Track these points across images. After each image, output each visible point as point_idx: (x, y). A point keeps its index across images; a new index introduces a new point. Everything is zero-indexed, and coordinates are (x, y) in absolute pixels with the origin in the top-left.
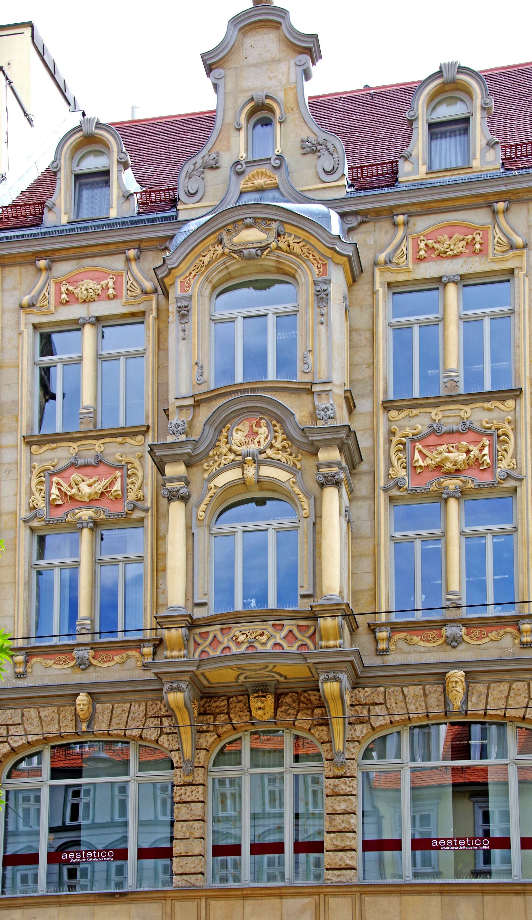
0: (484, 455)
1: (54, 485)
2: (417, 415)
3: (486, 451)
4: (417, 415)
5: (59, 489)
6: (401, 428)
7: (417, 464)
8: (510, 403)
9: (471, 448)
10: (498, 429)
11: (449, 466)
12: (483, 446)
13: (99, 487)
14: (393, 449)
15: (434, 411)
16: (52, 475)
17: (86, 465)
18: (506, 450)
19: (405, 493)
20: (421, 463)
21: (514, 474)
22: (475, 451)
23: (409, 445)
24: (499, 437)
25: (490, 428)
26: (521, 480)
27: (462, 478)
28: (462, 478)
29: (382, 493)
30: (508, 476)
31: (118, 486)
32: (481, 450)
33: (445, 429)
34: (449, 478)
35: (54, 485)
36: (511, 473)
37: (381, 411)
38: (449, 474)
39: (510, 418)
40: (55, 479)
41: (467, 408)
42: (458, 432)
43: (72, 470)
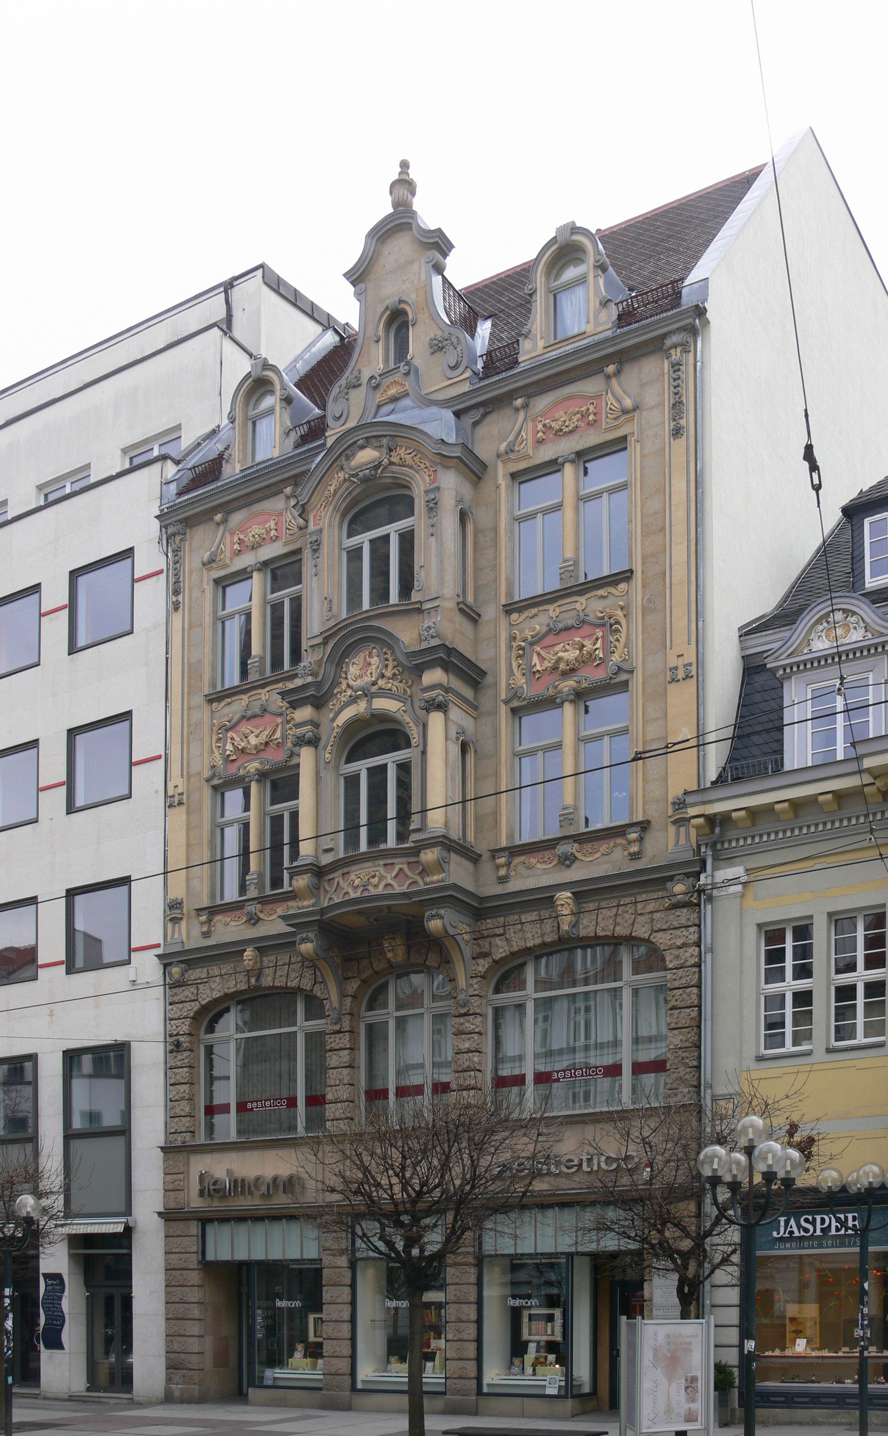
0: (596, 649)
1: (229, 740)
2: (535, 615)
3: (599, 645)
4: (535, 615)
5: (233, 744)
6: (521, 631)
7: (535, 670)
8: (623, 586)
9: (585, 643)
10: (610, 618)
12: (597, 639)
13: (263, 738)
14: (514, 653)
15: (551, 607)
16: (227, 730)
17: (254, 716)
18: (618, 640)
19: (525, 703)
20: (538, 668)
21: (624, 666)
22: (588, 645)
23: (528, 650)
24: (611, 626)
25: (603, 618)
27: (575, 678)
28: (575, 678)
29: (503, 706)
31: (278, 734)
32: (595, 644)
33: (561, 625)
34: (565, 680)
35: (229, 740)
36: (623, 665)
37: (503, 616)
38: (565, 674)
39: (621, 603)
40: (230, 734)
41: (582, 599)
42: (573, 627)
43: (244, 722)
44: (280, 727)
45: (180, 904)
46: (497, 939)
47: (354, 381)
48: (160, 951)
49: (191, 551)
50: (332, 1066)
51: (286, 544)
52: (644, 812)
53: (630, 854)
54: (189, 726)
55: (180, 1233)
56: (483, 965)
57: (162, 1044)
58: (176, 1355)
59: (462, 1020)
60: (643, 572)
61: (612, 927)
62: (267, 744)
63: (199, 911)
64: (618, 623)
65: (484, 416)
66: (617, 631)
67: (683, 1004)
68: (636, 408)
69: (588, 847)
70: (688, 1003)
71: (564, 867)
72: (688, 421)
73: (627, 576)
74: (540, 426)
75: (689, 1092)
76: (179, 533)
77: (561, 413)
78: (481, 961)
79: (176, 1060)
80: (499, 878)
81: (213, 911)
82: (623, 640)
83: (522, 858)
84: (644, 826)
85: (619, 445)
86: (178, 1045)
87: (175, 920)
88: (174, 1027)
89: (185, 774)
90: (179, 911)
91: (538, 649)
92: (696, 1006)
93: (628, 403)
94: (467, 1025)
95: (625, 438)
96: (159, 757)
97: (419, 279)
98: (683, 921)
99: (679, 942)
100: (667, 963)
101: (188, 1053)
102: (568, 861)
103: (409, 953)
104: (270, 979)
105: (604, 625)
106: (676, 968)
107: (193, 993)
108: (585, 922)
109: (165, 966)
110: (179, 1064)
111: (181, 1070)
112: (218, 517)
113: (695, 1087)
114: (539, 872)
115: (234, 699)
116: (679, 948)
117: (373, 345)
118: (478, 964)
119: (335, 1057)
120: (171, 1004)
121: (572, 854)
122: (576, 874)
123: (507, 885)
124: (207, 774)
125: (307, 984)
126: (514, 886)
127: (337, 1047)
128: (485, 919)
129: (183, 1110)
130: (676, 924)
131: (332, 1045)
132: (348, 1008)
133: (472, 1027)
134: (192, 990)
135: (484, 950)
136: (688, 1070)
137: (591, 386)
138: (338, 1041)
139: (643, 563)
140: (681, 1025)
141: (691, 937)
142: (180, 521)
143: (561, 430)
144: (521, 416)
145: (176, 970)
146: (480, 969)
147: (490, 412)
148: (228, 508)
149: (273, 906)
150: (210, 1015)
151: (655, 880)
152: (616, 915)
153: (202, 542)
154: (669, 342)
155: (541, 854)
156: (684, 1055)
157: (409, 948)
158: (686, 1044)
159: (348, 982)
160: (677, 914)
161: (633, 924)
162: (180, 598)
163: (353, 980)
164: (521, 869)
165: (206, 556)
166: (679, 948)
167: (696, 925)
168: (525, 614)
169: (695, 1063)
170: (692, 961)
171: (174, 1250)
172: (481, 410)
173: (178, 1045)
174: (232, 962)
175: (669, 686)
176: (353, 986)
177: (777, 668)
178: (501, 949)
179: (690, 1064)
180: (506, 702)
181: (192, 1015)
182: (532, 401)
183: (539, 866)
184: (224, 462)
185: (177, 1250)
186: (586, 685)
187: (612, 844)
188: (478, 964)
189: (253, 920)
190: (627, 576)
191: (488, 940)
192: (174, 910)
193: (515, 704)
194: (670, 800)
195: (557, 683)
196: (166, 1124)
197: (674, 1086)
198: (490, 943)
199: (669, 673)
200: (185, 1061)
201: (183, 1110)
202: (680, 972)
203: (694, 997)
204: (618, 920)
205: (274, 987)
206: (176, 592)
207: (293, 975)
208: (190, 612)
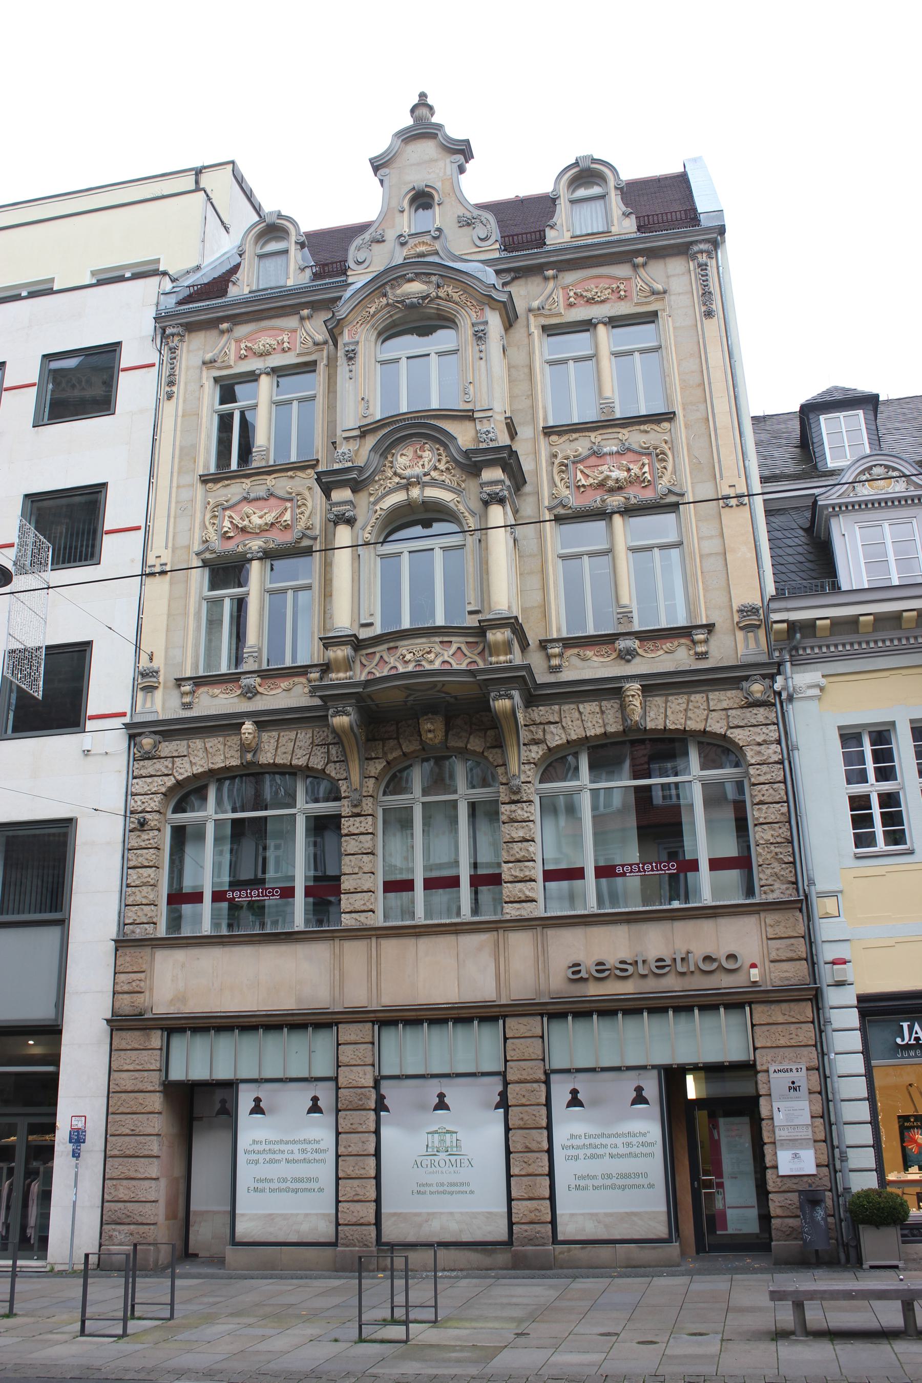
0: (644, 473)
1: (227, 518)
2: (576, 439)
3: (646, 469)
4: (576, 439)
5: (231, 522)
7: (580, 484)
9: (631, 466)
11: (610, 483)
12: (643, 465)
13: (269, 518)
14: (555, 470)
15: (593, 435)
16: (225, 509)
17: (257, 499)
19: (570, 511)
20: (583, 482)
22: (635, 469)
23: (571, 466)
24: (657, 455)
31: (287, 516)
32: (641, 469)
34: (613, 496)
35: (227, 518)
38: (611, 491)
40: (228, 513)
41: (625, 431)
43: (244, 503)
44: (289, 510)
45: (157, 672)
46: (552, 726)
47: (379, 237)
48: (127, 720)
49: (188, 351)
50: (349, 852)
51: (299, 355)
52: (707, 617)
53: (696, 654)
54: (177, 502)
55: (137, 1046)
56: (536, 752)
57: (122, 818)
58: (121, 1205)
59: (513, 807)
60: (684, 416)
61: (683, 721)
62: (272, 524)
63: (179, 682)
64: (663, 453)
65: (513, 279)
66: (664, 460)
67: (770, 800)
68: (665, 292)
69: (650, 644)
70: (777, 799)
71: (623, 662)
72: (716, 306)
73: (669, 417)
74: (572, 294)
75: (787, 889)
76: (179, 334)
77: (593, 286)
78: (534, 748)
79: (139, 840)
80: (550, 667)
81: (199, 682)
82: (670, 468)
83: (575, 651)
84: (710, 628)
85: (651, 317)
86: (142, 824)
87: (150, 689)
88: (139, 803)
89: (170, 545)
90: (155, 680)
91: (582, 467)
92: (784, 802)
93: (659, 287)
94: (520, 812)
95: (655, 314)
96: (138, 528)
97: (445, 172)
98: (761, 719)
99: (759, 739)
100: (749, 758)
101: (156, 833)
102: (627, 656)
103: (446, 735)
104: (269, 755)
105: (650, 454)
106: (758, 764)
107: (167, 767)
108: (652, 714)
109: (132, 737)
110: (143, 844)
111: (146, 851)
112: (225, 326)
113: (793, 883)
114: (596, 665)
115: (233, 481)
116: (759, 744)
117: (398, 215)
118: (530, 751)
119: (353, 842)
120: (134, 778)
121: (635, 649)
122: (638, 667)
123: (559, 675)
124: (197, 547)
125: (317, 762)
126: (567, 675)
127: (356, 832)
128: (537, 706)
129: (145, 897)
130: (754, 722)
131: (350, 829)
132: (371, 790)
133: (526, 815)
134: (166, 763)
135: (537, 737)
136: (784, 866)
137: (622, 271)
138: (357, 825)
140: (770, 821)
141: (771, 734)
142: (181, 325)
143: (593, 299)
144: (551, 284)
145: (147, 742)
146: (533, 755)
147: (519, 278)
148: (236, 319)
149: (277, 681)
150: (187, 793)
151: (728, 678)
152: (686, 710)
153: (196, 349)
154: (695, 248)
155: (597, 648)
156: (777, 850)
157: (448, 729)
158: (779, 840)
159: (371, 762)
160: (755, 712)
161: (706, 720)
162: (175, 389)
163: (377, 761)
164: (575, 661)
165: (208, 357)
166: (759, 744)
167: (774, 724)
169: (791, 859)
170: (776, 758)
171: (126, 1067)
172: (513, 274)
173: (142, 824)
174: (220, 736)
175: (723, 511)
176: (375, 768)
177: (827, 506)
178: (556, 737)
179: (786, 860)
181: (163, 790)
182: (561, 275)
183: (595, 658)
184: (230, 284)
185: (131, 1067)
187: (676, 643)
188: (530, 751)
189: (250, 693)
190: (669, 417)
191: (542, 727)
192: (146, 681)
194: (735, 608)
196: (120, 913)
197: (769, 882)
198: (544, 731)
200: (151, 841)
201: (145, 897)
202: (765, 768)
203: (783, 793)
204: (690, 714)
205: (274, 764)
206: (171, 383)
207: (299, 753)
208: (184, 401)
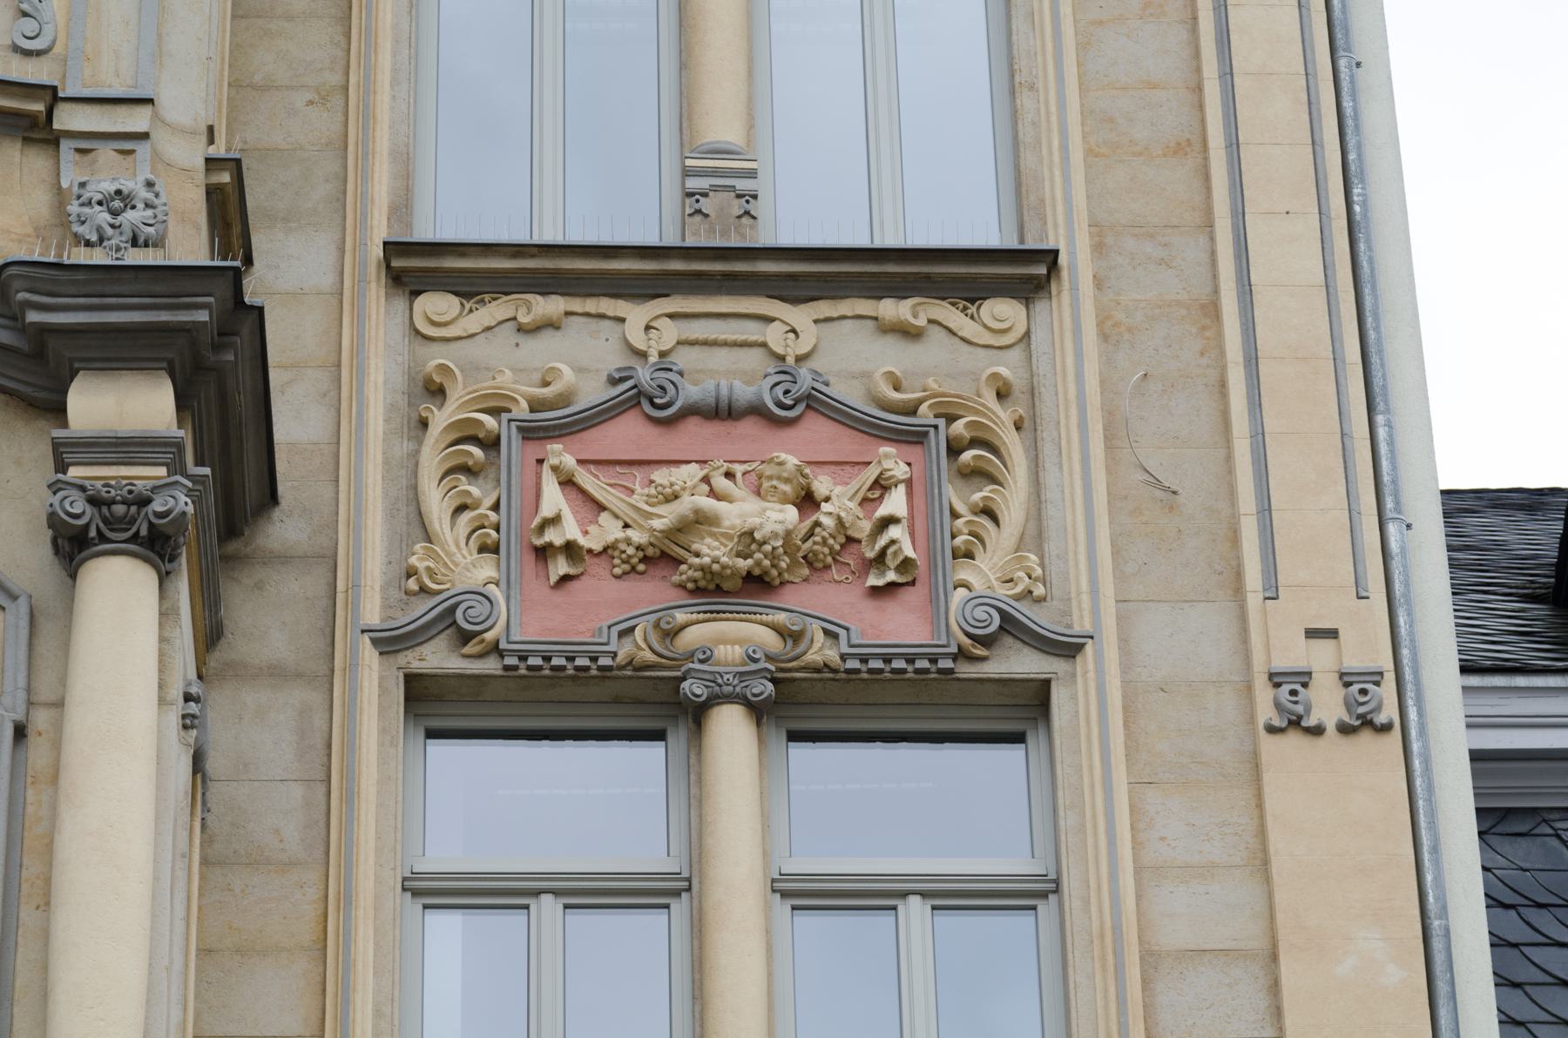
2: (551, 325)
3: (895, 504)
4: (551, 325)
7: (553, 537)
8: (1003, 311)
9: (821, 485)
10: (951, 419)
11: (712, 551)
12: (881, 486)
14: (432, 458)
18: (989, 513)
19: (491, 666)
20: (571, 530)
22: (840, 500)
23: (511, 443)
24: (954, 450)
26: (1069, 650)
28: (781, 617)
30: (1010, 626)
34: (715, 615)
36: (1025, 612)
37: (376, 290)
38: (713, 590)
41: (800, 315)
42: (757, 411)
60: (1099, 283)
73: (1024, 272)
91: (569, 461)
139: (1099, 248)
168: (495, 310)
180: (389, 643)
186: (832, 655)
190: (1024, 272)
193: (437, 657)
195: (681, 617)
199: (1264, 697)
